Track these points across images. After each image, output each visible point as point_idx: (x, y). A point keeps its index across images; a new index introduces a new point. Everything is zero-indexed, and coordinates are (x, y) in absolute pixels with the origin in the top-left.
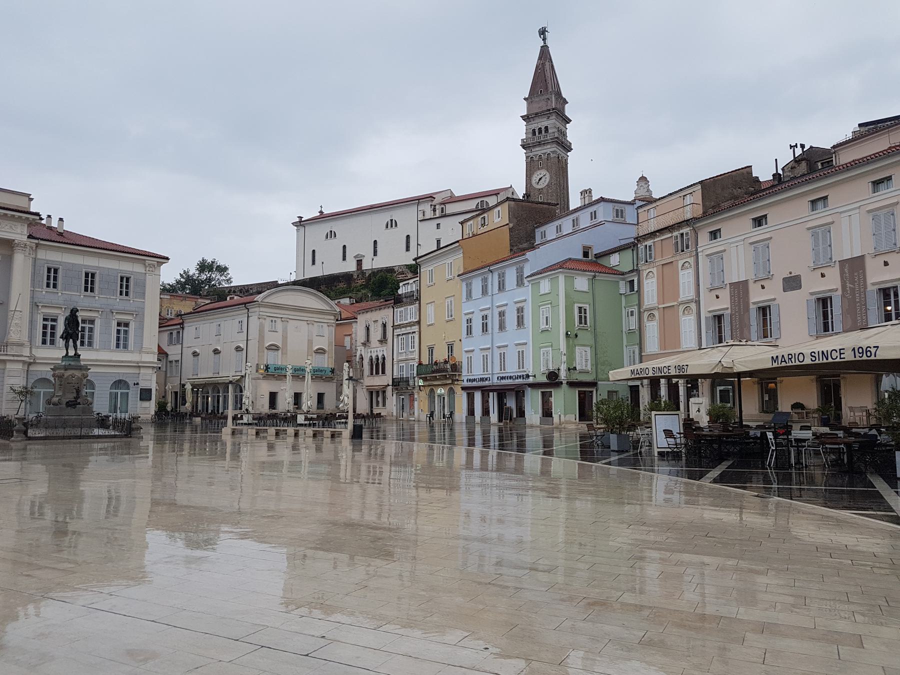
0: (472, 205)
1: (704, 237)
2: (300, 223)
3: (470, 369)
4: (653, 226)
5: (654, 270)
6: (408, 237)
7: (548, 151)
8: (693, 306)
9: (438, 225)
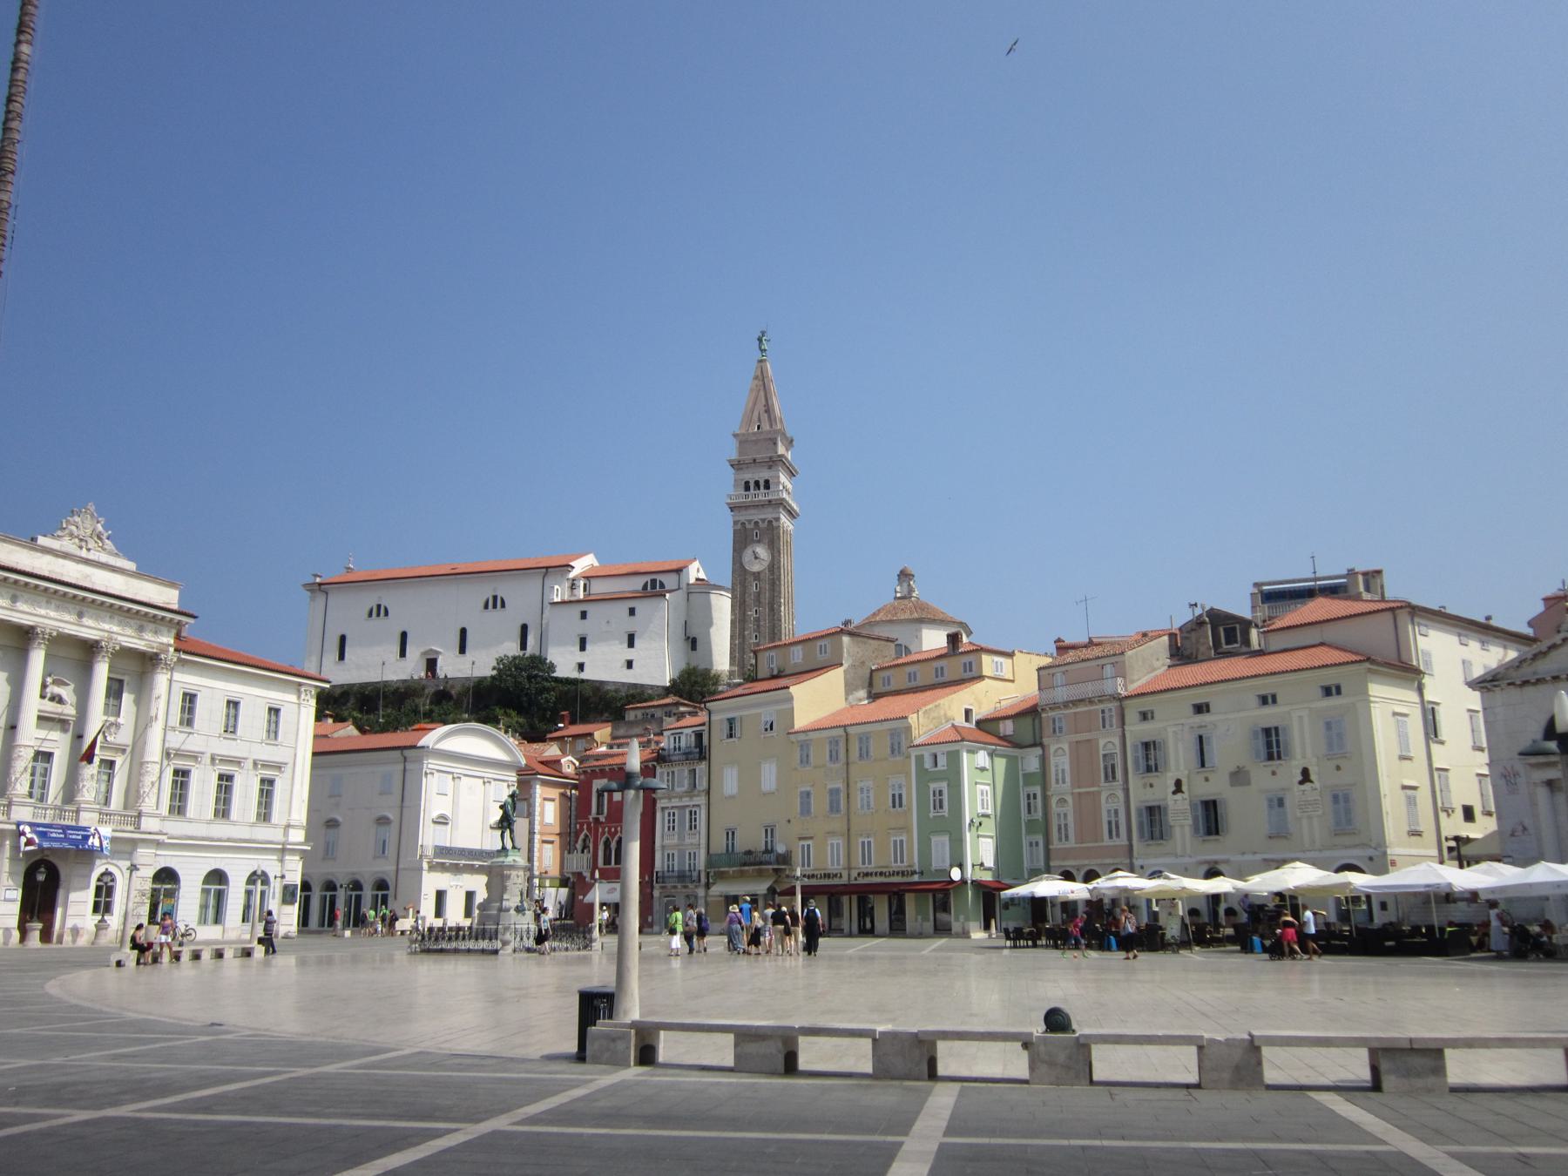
0: (637, 584)
1: (1132, 716)
2: (320, 588)
3: (806, 861)
4: (1061, 694)
5: (1066, 747)
6: (524, 628)
7: (769, 516)
8: (1120, 794)
9: (584, 615)
